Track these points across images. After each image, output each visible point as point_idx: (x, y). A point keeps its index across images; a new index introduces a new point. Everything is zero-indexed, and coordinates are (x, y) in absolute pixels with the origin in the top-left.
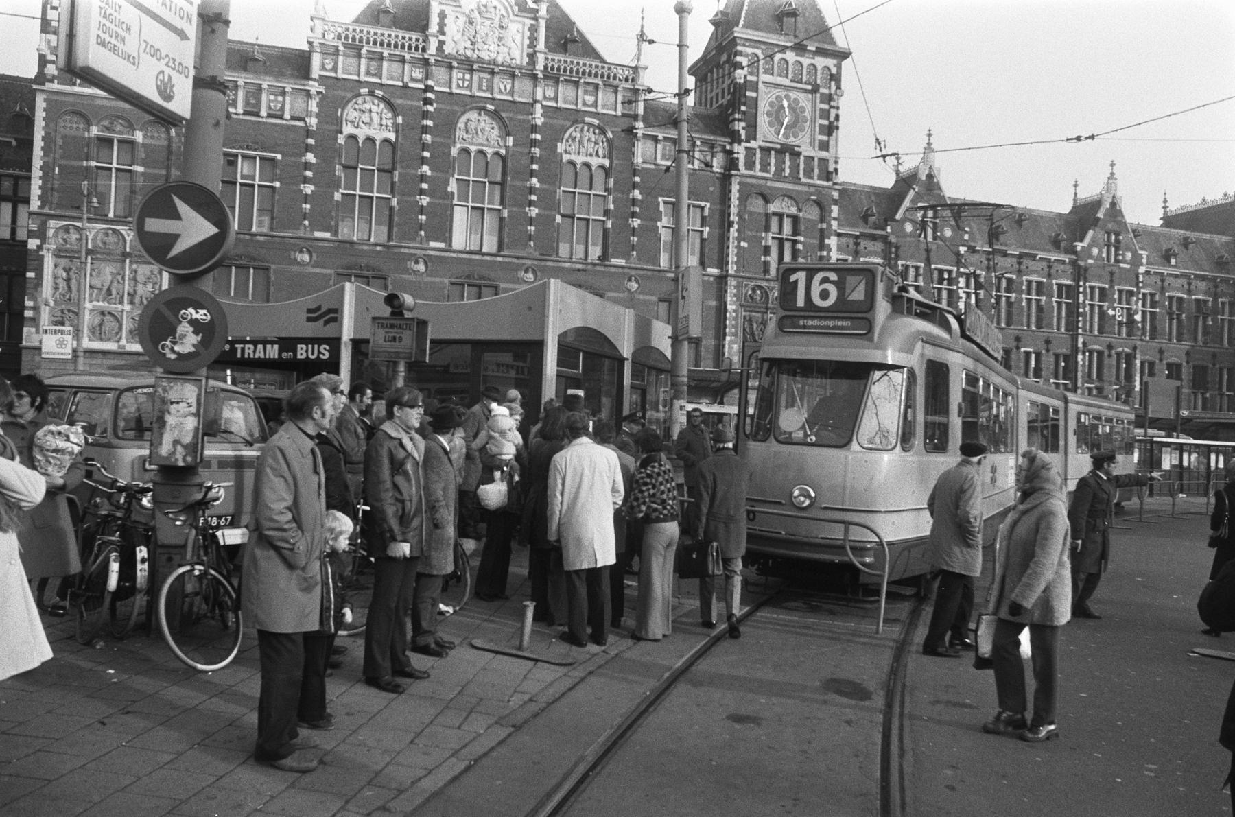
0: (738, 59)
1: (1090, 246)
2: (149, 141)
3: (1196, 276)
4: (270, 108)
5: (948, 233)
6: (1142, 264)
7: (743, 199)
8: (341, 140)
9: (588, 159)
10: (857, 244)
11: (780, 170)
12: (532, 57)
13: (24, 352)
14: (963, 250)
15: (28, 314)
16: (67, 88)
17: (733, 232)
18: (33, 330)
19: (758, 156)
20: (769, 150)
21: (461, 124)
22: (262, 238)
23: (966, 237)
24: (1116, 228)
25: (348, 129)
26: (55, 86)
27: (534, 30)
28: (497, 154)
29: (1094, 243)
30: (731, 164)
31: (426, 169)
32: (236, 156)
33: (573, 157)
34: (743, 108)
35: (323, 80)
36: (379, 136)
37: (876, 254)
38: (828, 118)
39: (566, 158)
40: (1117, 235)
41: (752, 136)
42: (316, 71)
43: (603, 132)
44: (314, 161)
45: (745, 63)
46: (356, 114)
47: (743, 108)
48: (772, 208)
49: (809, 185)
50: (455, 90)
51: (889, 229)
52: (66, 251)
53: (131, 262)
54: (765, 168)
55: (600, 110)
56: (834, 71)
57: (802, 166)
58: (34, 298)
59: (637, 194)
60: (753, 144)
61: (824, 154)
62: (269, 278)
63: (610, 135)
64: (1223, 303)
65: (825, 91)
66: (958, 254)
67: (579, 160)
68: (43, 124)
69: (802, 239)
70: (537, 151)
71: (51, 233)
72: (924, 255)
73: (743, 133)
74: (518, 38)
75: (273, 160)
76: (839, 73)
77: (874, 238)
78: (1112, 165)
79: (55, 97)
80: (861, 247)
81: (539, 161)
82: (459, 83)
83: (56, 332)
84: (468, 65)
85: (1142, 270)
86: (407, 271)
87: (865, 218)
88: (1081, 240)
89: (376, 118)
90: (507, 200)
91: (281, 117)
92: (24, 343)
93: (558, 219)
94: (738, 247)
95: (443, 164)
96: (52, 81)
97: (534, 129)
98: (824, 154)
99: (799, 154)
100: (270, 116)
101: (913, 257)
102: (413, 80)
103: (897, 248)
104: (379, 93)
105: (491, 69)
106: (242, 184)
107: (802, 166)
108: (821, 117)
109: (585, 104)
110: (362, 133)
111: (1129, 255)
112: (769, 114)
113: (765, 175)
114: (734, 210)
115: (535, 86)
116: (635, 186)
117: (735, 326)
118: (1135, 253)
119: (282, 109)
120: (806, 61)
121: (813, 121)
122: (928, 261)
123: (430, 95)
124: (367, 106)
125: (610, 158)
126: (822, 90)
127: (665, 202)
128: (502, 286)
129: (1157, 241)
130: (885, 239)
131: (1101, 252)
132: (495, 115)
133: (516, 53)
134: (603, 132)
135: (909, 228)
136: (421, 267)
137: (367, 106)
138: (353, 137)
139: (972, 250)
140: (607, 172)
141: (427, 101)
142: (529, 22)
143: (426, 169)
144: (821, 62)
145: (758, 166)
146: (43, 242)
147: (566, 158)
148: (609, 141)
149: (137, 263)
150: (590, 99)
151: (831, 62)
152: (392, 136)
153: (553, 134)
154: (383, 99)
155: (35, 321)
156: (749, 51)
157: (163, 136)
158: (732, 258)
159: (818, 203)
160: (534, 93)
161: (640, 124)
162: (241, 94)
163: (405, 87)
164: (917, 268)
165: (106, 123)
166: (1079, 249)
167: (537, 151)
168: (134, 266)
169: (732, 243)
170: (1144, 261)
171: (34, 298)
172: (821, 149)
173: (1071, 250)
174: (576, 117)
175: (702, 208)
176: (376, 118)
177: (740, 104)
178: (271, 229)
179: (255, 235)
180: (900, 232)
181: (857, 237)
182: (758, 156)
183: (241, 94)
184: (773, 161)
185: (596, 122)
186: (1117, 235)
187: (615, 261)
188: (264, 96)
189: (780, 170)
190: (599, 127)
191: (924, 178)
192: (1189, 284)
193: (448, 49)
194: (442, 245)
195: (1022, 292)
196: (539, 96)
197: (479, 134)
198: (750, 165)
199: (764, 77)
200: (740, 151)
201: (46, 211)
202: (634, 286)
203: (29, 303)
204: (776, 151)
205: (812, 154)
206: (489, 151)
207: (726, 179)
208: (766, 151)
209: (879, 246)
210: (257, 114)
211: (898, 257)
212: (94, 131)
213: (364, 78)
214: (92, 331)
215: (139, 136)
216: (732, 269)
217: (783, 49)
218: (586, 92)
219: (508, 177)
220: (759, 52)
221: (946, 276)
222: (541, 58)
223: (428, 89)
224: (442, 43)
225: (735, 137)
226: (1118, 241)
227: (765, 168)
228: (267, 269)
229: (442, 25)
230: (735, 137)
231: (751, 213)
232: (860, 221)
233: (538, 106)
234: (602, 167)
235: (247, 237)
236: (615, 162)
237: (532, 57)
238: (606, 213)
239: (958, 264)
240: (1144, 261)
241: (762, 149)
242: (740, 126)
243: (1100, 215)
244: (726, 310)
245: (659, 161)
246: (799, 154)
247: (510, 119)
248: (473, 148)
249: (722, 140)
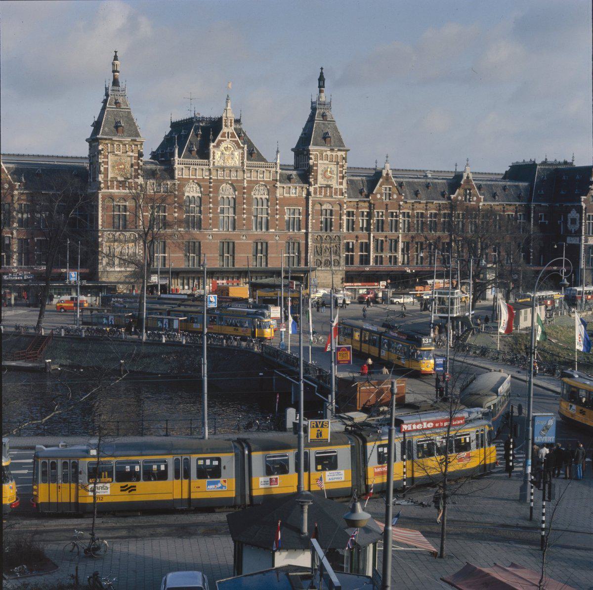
0: (311, 156)
1: (457, 196)
3: (506, 204)
5: (395, 196)
6: (481, 202)
7: (313, 205)
8: (185, 198)
9: (261, 196)
10: (357, 204)
11: (326, 193)
12: (243, 163)
14: (401, 203)
16: (107, 190)
17: (310, 217)
19: (318, 190)
20: (322, 187)
21: (221, 188)
23: (403, 198)
24: (469, 187)
25: (186, 194)
27: (243, 154)
28: (233, 198)
29: (459, 194)
30: (309, 194)
31: (211, 205)
33: (256, 196)
34: (313, 174)
35: (179, 179)
36: (196, 195)
37: (365, 208)
38: (342, 173)
39: (254, 196)
40: (470, 190)
41: (316, 183)
42: (177, 176)
43: (266, 186)
45: (313, 158)
46: (189, 189)
47: (313, 174)
48: (323, 207)
49: (335, 198)
50: (219, 178)
51: (370, 198)
54: (320, 194)
55: (265, 179)
56: (344, 156)
57: (333, 191)
59: (278, 207)
60: (316, 186)
61: (341, 187)
63: (268, 187)
64: (520, 215)
65: (341, 164)
66: (400, 205)
67: (259, 197)
69: (333, 217)
70: (245, 196)
72: (385, 206)
73: (313, 183)
74: (238, 157)
76: (346, 157)
77: (365, 202)
78: (468, 160)
80: (359, 206)
81: (247, 199)
82: (220, 175)
84: (223, 169)
85: (481, 204)
86: (207, 239)
87: (361, 192)
88: (454, 194)
89: (195, 189)
90: (236, 213)
93: (253, 218)
94: (312, 222)
95: (216, 203)
97: (244, 188)
98: (341, 187)
99: (332, 188)
101: (380, 208)
102: (206, 176)
103: (374, 205)
104: (196, 181)
105: (230, 169)
107: (333, 191)
108: (340, 173)
109: (260, 178)
110: (191, 195)
111: (475, 198)
112: (321, 174)
113: (321, 196)
114: (310, 209)
115: (244, 173)
116: (277, 204)
117: (312, 250)
118: (477, 197)
120: (334, 154)
121: (337, 175)
122: (387, 209)
123: (212, 181)
124: (192, 186)
125: (268, 195)
126: (340, 163)
127: (287, 209)
128: (236, 241)
129: (492, 189)
130: (369, 202)
131: (462, 198)
132: (232, 185)
133: (237, 162)
134: (266, 186)
135: (379, 196)
136: (211, 237)
137: (192, 186)
138: (188, 197)
139: (406, 202)
140: (268, 200)
141: (210, 183)
142: (241, 151)
143: (211, 205)
144: (340, 153)
145: (318, 193)
147: (254, 196)
148: (268, 190)
150: (262, 176)
151: (343, 153)
152: (200, 195)
153: (250, 189)
154: (197, 183)
156: (315, 153)
158: (310, 226)
159: (339, 204)
160: (244, 176)
161: (278, 183)
163: (203, 178)
164: (382, 212)
166: (452, 198)
167: (245, 196)
169: (310, 221)
170: (482, 200)
172: (340, 185)
173: (449, 198)
174: (257, 182)
175: (299, 210)
176: (195, 189)
177: (312, 172)
180: (375, 199)
181: (357, 202)
182: (318, 190)
184: (323, 191)
185: (264, 183)
186: (470, 190)
187: (271, 230)
189: (326, 193)
190: (264, 185)
191: (385, 175)
192: (504, 208)
193: (216, 164)
194: (217, 230)
195: (427, 218)
196: (245, 177)
197: (226, 191)
198: (315, 193)
199: (320, 162)
200: (312, 189)
202: (277, 238)
204: (324, 187)
205: (337, 187)
206: (230, 197)
207: (307, 199)
208: (321, 188)
209: (367, 204)
211: (374, 208)
213: (191, 177)
215: (127, 204)
216: (310, 230)
217: (326, 151)
218: (260, 174)
219: (235, 204)
220: (317, 153)
221: (395, 214)
222: (245, 163)
223: (210, 178)
224: (214, 162)
225: (310, 184)
226: (470, 193)
227: (320, 194)
229: (214, 156)
230: (310, 184)
231: (316, 210)
232: (359, 194)
233: (245, 181)
234: (266, 198)
236: (270, 196)
237: (243, 163)
238: (268, 214)
239: (399, 209)
240: (482, 200)
241: (319, 187)
242: (311, 180)
243: (462, 182)
244: (308, 244)
245: (285, 195)
246: (332, 188)
247: (237, 186)
248: (225, 197)
249: (306, 186)
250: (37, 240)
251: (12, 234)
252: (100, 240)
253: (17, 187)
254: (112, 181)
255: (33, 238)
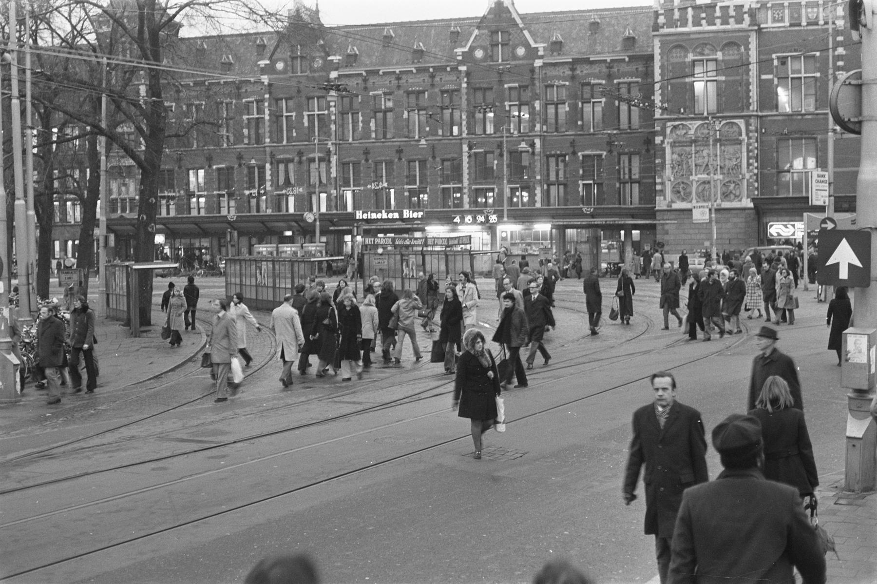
2: (727, 58)
4: (808, 18)
13: (658, 214)
15: (658, 187)
18: (662, 198)
22: (810, 117)
26: (666, 30)
32: (787, 57)
44: (844, 53)
52: (679, 142)
53: (721, 146)
58: (661, 177)
62: (817, 146)
68: (659, 57)
71: (668, 131)
75: (814, 56)
79: (664, 38)
83: (700, 207)
91: (817, 24)
92: (657, 208)
96: (663, 27)
100: (809, 24)
106: (792, 78)
119: (817, 17)
146: (665, 137)
149: (724, 145)
155: (662, 192)
157: (736, 52)
162: (787, 11)
165: (699, 50)
168: (723, 148)
171: (661, 177)
178: (816, 109)
179: (805, 115)
183: (787, 11)
188: (803, 11)
201: (665, 116)
203: (658, 180)
210: (799, 25)
212: (691, 57)
214: (698, 194)
228: (815, 139)
235: (799, 117)
250: (584, 156)
251: (533, 145)
252: (658, 140)
253: (541, 53)
254: (683, 10)
255: (574, 153)
